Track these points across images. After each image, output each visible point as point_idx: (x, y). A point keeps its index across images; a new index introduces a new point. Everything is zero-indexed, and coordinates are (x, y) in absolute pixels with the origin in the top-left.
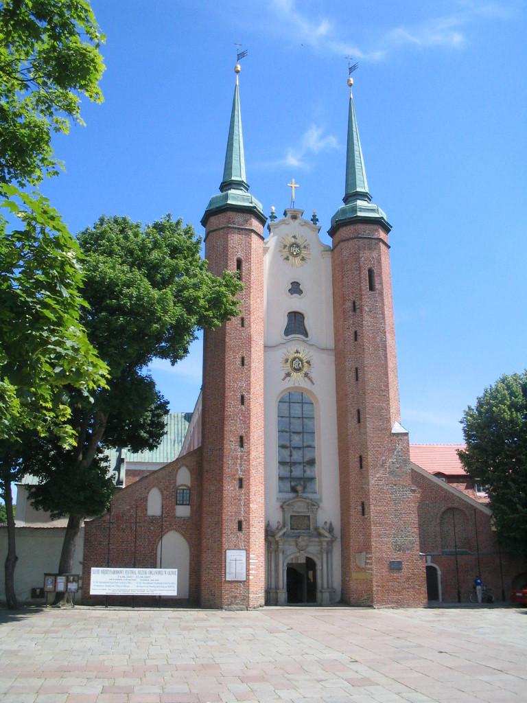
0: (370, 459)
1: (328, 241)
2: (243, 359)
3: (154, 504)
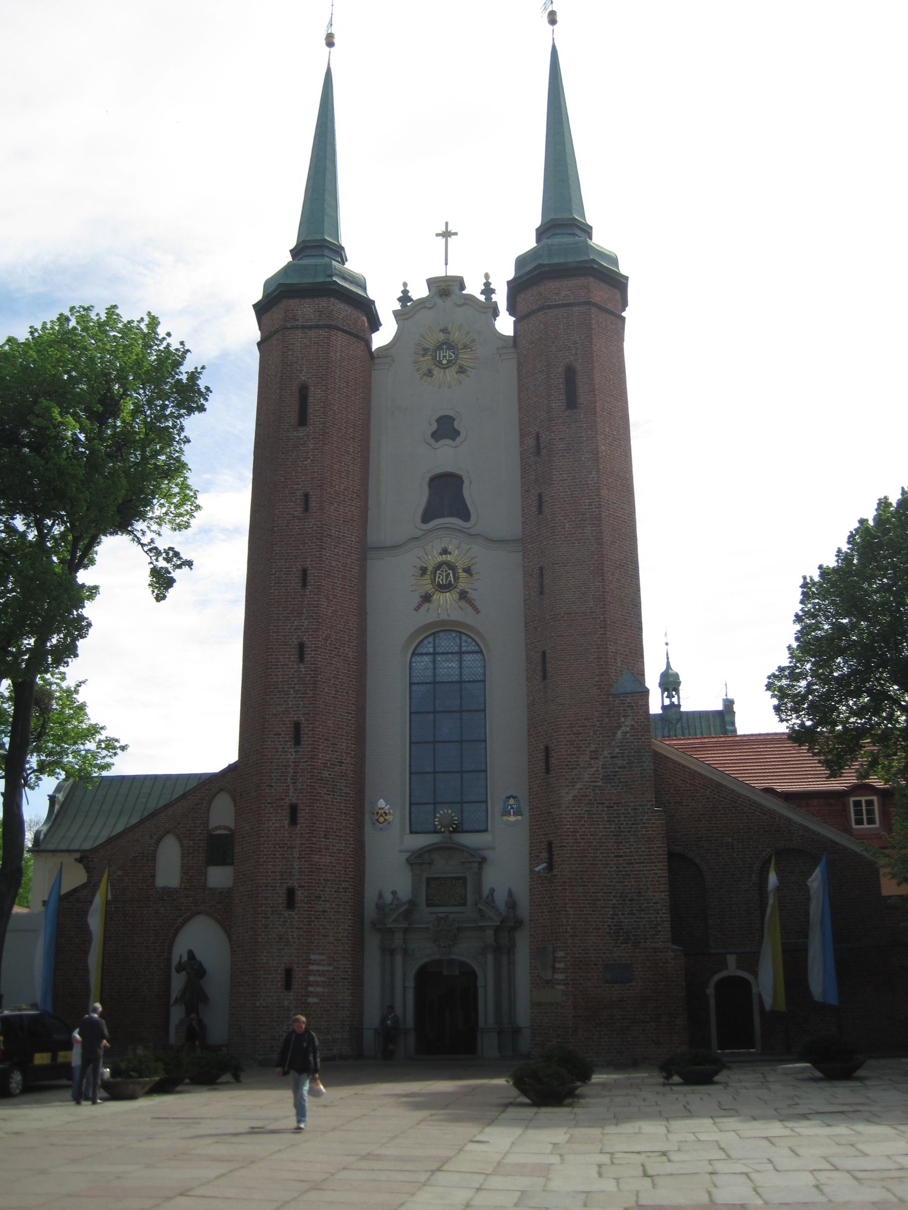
1: (505, 325)
2: (305, 572)
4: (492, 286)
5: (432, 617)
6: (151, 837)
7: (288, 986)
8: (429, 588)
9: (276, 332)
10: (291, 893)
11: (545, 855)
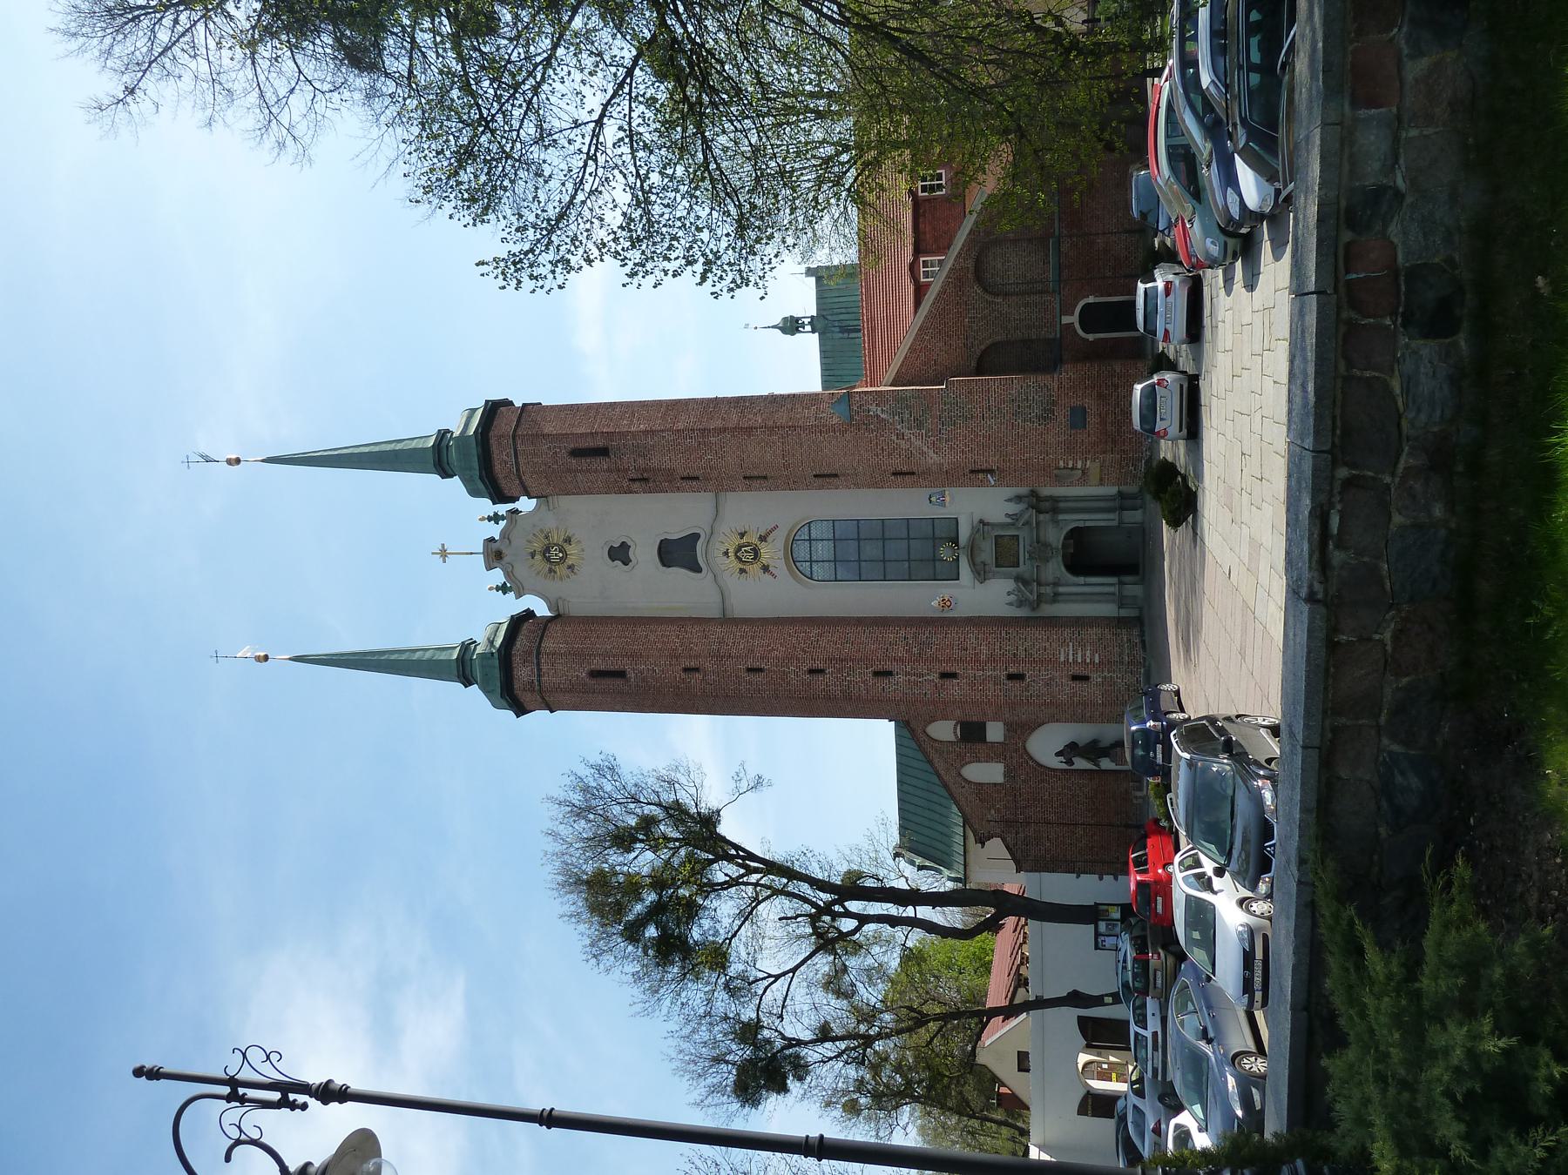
0: (897, 463)
1: (526, 504)
2: (749, 670)
3: (989, 772)
4: (492, 515)
5: (781, 564)
6: (964, 787)
7: (1086, 678)
8: (756, 567)
9: (543, 698)
10: (1011, 677)
11: (981, 476)
